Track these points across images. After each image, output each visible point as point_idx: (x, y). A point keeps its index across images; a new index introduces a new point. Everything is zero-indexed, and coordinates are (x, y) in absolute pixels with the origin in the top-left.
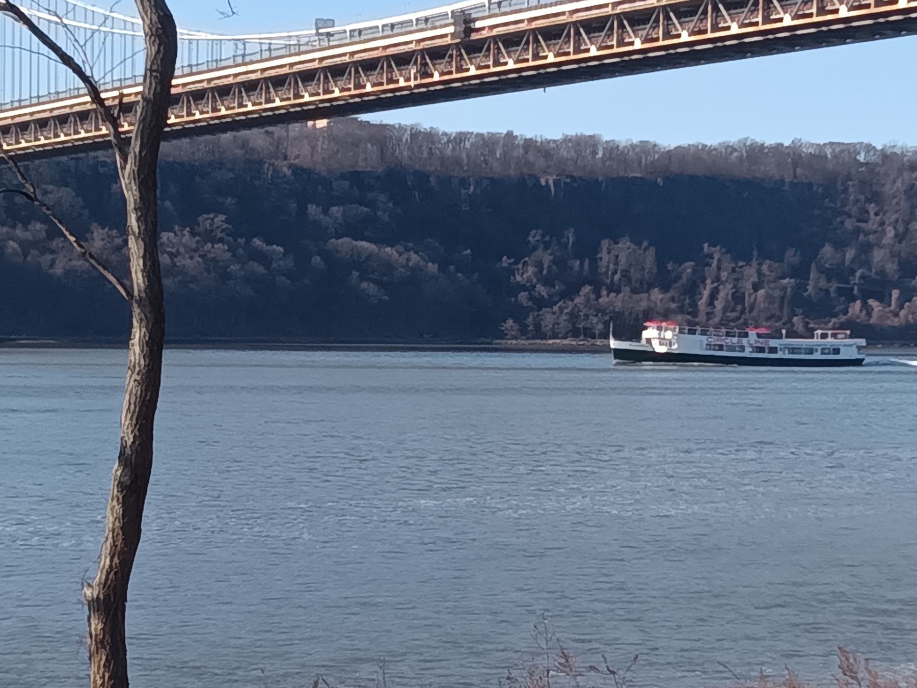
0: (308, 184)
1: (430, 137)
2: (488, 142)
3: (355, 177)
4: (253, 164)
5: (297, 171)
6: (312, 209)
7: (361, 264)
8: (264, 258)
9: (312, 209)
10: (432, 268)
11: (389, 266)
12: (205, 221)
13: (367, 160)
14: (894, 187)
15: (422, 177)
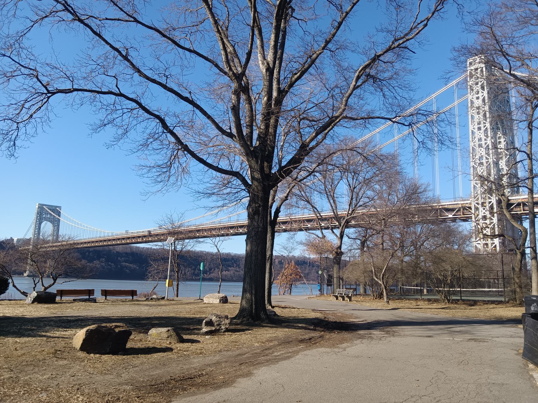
0: (118, 254)
1: (139, 247)
2: (148, 249)
3: (126, 253)
4: (110, 251)
5: (117, 252)
6: (119, 258)
7: (126, 267)
8: (110, 266)
9: (119, 258)
10: (138, 268)
11: (131, 267)
12: (101, 259)
13: (129, 251)
14: (209, 258)
15: (137, 254)
